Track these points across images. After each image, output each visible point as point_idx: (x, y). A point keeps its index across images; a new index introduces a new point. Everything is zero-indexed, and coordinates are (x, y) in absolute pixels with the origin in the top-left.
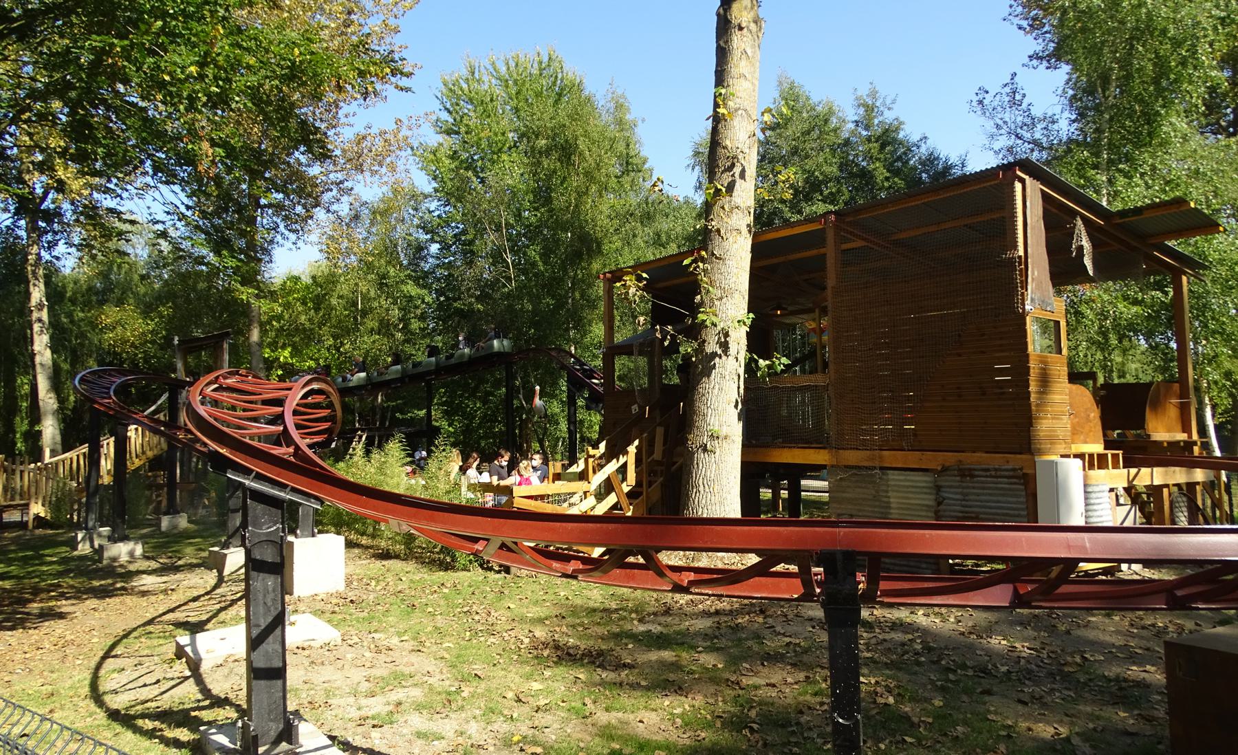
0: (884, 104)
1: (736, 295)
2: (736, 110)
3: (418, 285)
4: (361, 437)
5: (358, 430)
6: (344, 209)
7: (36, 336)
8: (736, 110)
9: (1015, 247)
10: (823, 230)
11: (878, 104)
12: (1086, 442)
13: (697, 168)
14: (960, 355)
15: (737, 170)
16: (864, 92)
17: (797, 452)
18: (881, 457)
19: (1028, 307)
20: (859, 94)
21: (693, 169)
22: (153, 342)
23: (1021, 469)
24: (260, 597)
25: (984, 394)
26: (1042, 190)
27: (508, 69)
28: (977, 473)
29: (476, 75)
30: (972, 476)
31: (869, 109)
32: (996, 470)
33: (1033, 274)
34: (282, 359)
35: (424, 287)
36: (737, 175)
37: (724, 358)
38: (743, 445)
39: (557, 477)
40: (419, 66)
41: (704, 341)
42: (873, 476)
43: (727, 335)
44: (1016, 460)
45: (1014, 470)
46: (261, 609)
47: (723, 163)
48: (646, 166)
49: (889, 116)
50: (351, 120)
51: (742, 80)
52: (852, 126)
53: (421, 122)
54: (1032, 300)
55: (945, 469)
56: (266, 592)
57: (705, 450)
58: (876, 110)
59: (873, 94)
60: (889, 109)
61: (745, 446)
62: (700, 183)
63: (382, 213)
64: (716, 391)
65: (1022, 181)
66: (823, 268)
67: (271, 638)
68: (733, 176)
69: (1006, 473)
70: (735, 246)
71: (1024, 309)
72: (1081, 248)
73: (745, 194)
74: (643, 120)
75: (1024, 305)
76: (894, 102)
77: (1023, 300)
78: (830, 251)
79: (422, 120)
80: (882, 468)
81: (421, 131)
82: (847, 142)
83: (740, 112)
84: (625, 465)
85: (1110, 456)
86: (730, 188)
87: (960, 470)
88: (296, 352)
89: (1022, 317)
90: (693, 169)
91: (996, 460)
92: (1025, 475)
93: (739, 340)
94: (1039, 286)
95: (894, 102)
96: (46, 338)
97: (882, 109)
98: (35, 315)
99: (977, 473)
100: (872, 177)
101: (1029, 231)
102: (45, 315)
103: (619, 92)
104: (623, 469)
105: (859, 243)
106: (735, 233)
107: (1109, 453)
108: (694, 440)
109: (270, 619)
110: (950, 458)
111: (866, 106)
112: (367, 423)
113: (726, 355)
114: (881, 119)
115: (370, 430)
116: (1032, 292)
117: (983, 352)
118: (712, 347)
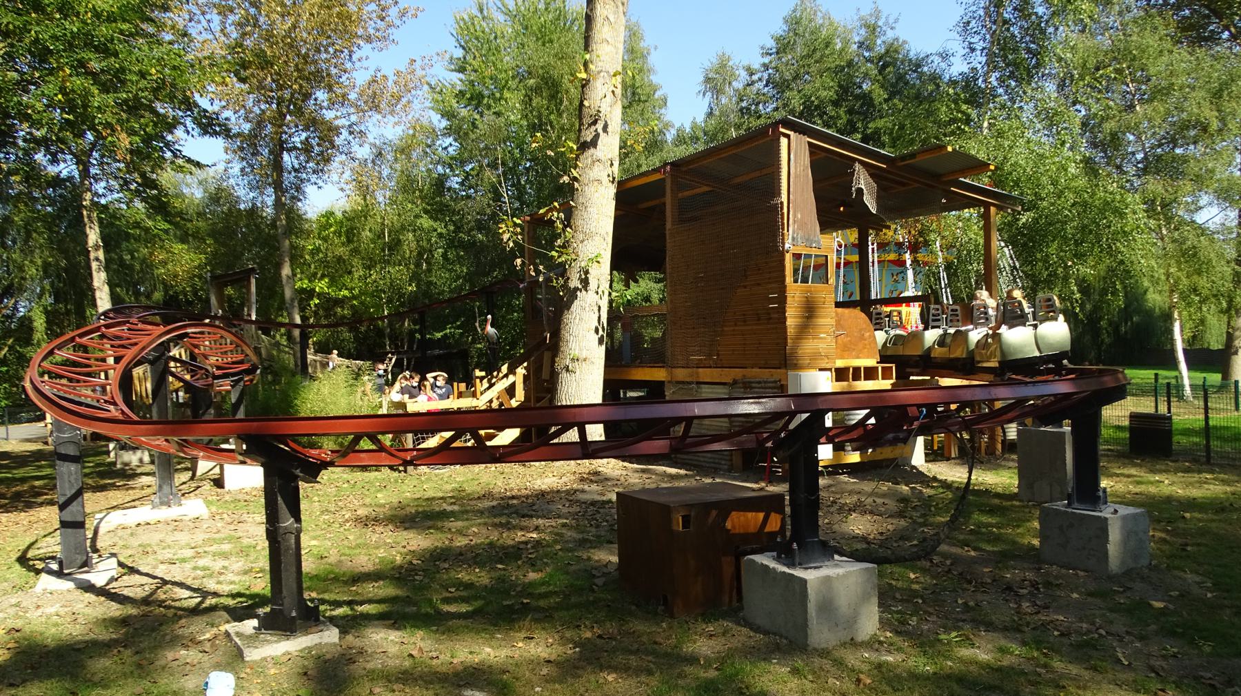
0: (886, 23)
1: (597, 238)
2: (599, 72)
3: (431, 218)
4: (391, 359)
5: (388, 353)
6: (363, 152)
7: (95, 274)
8: (599, 72)
9: (779, 194)
10: (663, 180)
11: (880, 23)
12: (858, 357)
13: (709, 94)
14: (745, 287)
15: (600, 126)
16: (866, 11)
17: (647, 370)
18: (697, 373)
19: (787, 246)
20: (863, 13)
21: (704, 94)
22: (200, 277)
23: (780, 381)
24: (66, 477)
25: (759, 320)
26: (809, 143)
27: (516, 4)
28: (754, 385)
29: (485, 12)
30: (752, 388)
31: (873, 29)
32: (765, 382)
33: (795, 216)
34: (317, 289)
35: (435, 220)
36: (600, 131)
37: (584, 292)
38: (606, 366)
39: (460, 395)
40: (421, 8)
41: (568, 278)
42: (692, 389)
43: (587, 272)
44: (777, 374)
45: (775, 382)
46: (67, 485)
47: (586, 121)
48: (658, 94)
49: (890, 35)
50: (365, 63)
51: (605, 44)
52: (855, 47)
53: (433, 62)
54: (793, 239)
55: (735, 382)
56: (70, 474)
57: (568, 370)
58: (879, 30)
59: (877, 13)
60: (892, 28)
61: (607, 366)
62: (712, 109)
63: (404, 150)
64: (577, 321)
65: (788, 136)
66: (663, 212)
67: (75, 503)
68: (596, 130)
69: (771, 385)
70: (596, 194)
71: (783, 247)
72: (860, 191)
73: (609, 147)
74: (656, 48)
75: (783, 244)
76: (896, 21)
77: (783, 239)
78: (668, 199)
79: (434, 59)
80: (698, 383)
81: (433, 71)
82: (850, 64)
83: (602, 74)
84: (513, 385)
85: (880, 369)
86: (594, 143)
87: (744, 383)
88: (333, 282)
89: (782, 255)
90: (704, 94)
91: (765, 374)
92: (782, 385)
93: (601, 273)
94: (802, 225)
95: (896, 21)
96: (103, 275)
97: (884, 28)
98: (92, 255)
99: (754, 385)
100: (871, 99)
101: (791, 180)
102: (101, 254)
103: (634, 20)
104: (511, 391)
105: (706, 189)
106: (596, 183)
107: (880, 366)
108: (563, 361)
109: (73, 491)
110: (737, 373)
111: (867, 26)
112: (397, 347)
113: (586, 291)
114: (883, 38)
115: (398, 353)
116: (794, 232)
117: (759, 284)
118: (574, 283)
